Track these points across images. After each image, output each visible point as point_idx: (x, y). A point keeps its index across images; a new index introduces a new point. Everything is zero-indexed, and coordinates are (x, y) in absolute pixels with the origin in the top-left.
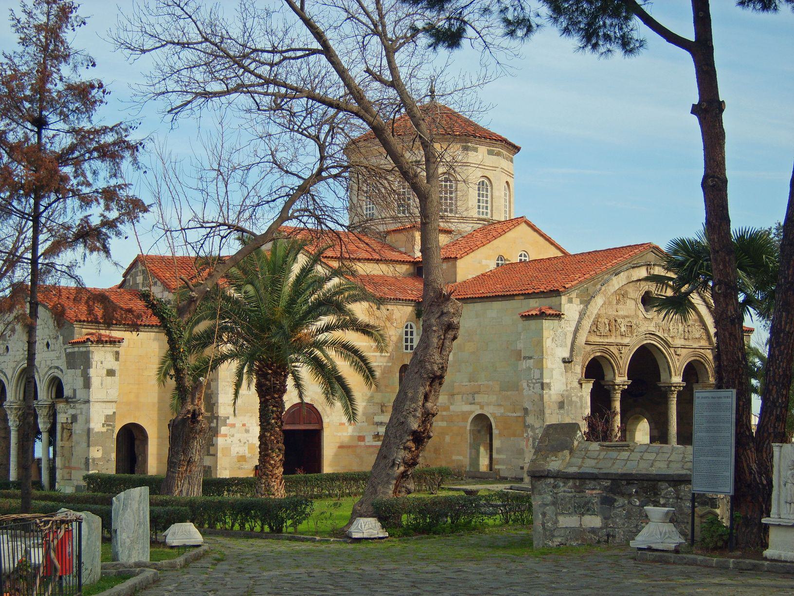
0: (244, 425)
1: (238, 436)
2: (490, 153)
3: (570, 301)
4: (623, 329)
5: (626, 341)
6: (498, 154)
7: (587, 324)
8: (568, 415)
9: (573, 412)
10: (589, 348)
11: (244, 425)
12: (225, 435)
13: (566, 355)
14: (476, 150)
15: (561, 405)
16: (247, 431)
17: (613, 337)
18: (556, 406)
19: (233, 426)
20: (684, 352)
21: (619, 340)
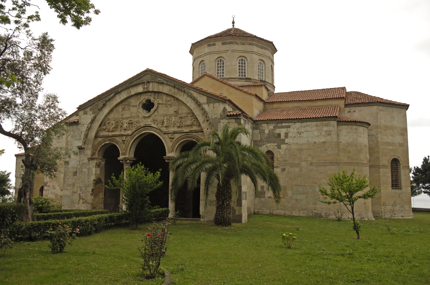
0: (53, 186)
1: (51, 190)
2: (223, 44)
3: (86, 113)
4: (125, 125)
5: (126, 133)
6: (229, 43)
7: (96, 125)
8: (79, 179)
9: (83, 177)
10: (100, 139)
11: (53, 186)
12: (46, 190)
13: (80, 144)
14: (214, 45)
15: (75, 174)
16: (54, 188)
17: (119, 131)
18: (72, 174)
19: (49, 186)
20: (177, 136)
21: (123, 133)
